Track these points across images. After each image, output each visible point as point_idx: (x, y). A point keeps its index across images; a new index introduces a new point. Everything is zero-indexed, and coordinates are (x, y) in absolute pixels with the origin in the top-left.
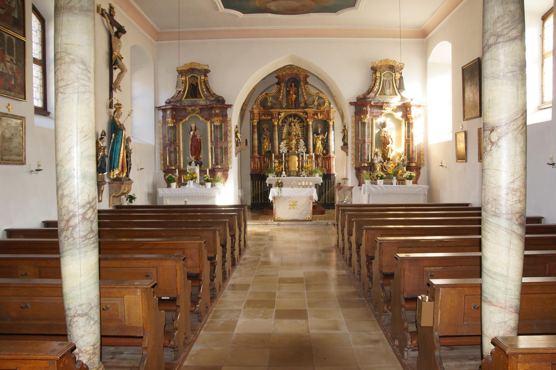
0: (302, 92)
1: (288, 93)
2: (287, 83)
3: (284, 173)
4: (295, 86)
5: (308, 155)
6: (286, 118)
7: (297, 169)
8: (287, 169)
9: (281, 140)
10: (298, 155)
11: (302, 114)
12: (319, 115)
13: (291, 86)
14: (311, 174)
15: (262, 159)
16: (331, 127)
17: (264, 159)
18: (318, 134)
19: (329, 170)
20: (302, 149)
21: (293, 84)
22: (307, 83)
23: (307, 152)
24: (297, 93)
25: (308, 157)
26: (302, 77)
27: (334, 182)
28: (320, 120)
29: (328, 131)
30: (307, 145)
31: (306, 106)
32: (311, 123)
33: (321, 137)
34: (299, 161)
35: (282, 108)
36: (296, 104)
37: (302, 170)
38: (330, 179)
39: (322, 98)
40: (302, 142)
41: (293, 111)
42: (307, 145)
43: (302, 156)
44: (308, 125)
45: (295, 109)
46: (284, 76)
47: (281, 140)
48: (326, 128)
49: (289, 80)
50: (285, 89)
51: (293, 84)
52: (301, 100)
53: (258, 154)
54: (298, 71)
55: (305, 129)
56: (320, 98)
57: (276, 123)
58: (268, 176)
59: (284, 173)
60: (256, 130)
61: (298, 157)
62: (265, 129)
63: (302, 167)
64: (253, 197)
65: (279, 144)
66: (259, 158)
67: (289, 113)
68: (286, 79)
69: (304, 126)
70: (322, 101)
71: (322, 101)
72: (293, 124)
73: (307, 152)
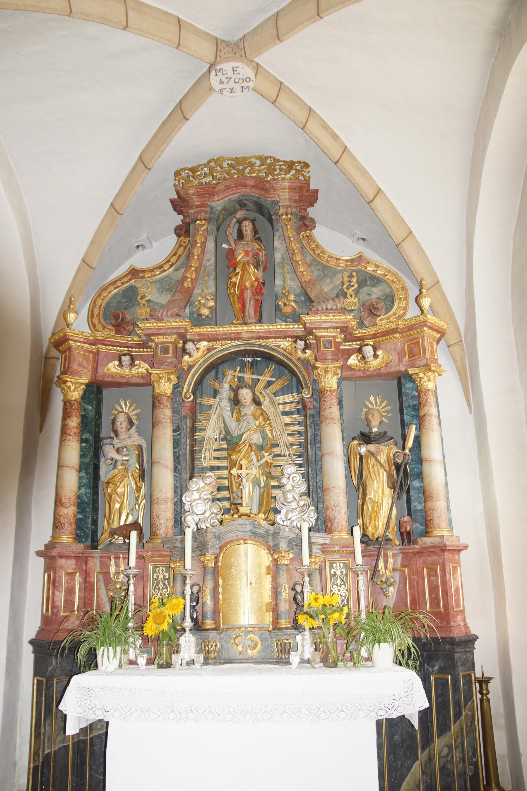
0: (290, 252)
1: (229, 262)
2: (219, 223)
3: (188, 642)
4: (255, 231)
5: (320, 538)
6: (215, 368)
7: (268, 618)
8: (207, 624)
9: (187, 467)
10: (270, 541)
11: (286, 344)
12: (368, 351)
13: (240, 236)
14: (341, 647)
15: (95, 564)
16: (431, 399)
17: (105, 566)
18: (366, 438)
19: (444, 616)
20: (295, 514)
21: (247, 227)
22: (305, 223)
23: (323, 524)
24: (266, 265)
25: (325, 549)
26: (283, 196)
27: (468, 679)
28: (378, 375)
29: (420, 420)
30: (316, 492)
31: (308, 302)
32: (330, 382)
33: (385, 452)
34: (275, 569)
35: (198, 320)
36: (262, 302)
37: (296, 626)
38: (449, 667)
39: (375, 280)
40: (293, 479)
41: (249, 332)
42: (316, 492)
43: (295, 544)
44: (319, 394)
45: (260, 321)
46: (208, 191)
47: (187, 467)
48: (409, 403)
49: (229, 212)
50: (211, 245)
51: (247, 227)
52: (285, 282)
53: (78, 538)
54: (271, 169)
55: (310, 419)
56: (368, 280)
57: (165, 388)
58: (91, 663)
59: (188, 642)
60: (74, 422)
61: (273, 549)
62: (121, 422)
63: (297, 601)
64: (36, 768)
65: (180, 489)
66: (82, 560)
67: (232, 346)
68: (218, 203)
69: (303, 407)
70: (377, 292)
71: (377, 292)
72: (246, 394)
73: (323, 524)
